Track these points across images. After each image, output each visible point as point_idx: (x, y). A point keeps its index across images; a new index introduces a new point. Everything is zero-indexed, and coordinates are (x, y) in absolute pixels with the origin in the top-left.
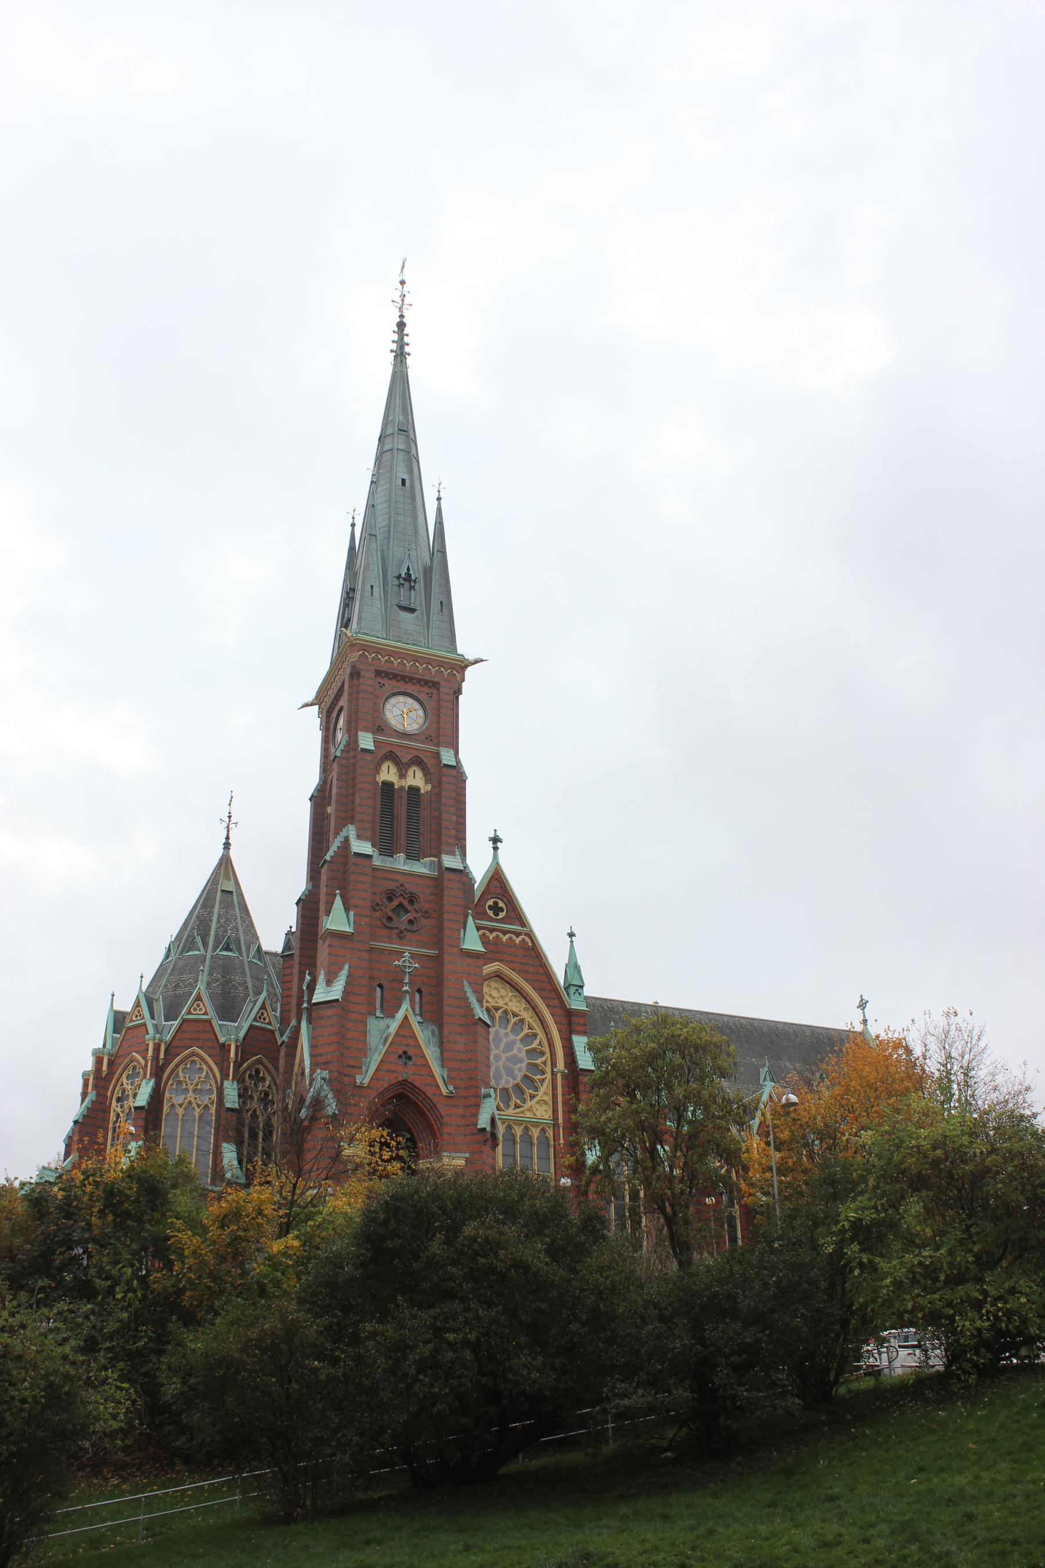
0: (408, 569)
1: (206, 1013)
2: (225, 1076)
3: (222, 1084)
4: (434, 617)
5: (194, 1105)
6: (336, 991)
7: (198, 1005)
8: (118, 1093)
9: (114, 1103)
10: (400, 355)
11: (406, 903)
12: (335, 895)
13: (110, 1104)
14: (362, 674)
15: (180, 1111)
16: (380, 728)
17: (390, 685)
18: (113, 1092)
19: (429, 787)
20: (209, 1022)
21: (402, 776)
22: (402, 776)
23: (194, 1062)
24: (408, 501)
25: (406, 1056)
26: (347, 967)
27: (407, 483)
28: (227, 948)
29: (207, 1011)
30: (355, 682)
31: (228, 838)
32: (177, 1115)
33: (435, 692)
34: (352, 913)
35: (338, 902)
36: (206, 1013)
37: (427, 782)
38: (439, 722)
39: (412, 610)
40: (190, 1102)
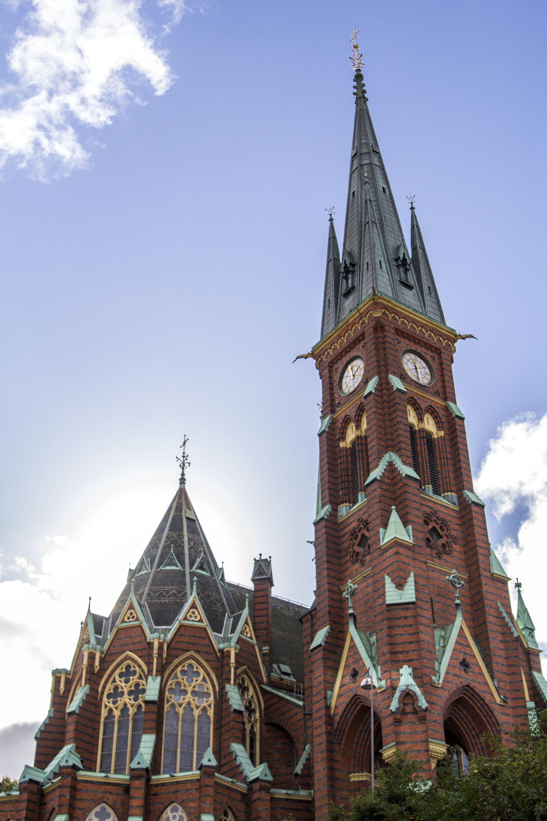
0: (404, 254)
1: (201, 621)
2: (223, 679)
3: (222, 688)
4: (427, 297)
5: (193, 706)
6: (409, 594)
7: (194, 613)
8: (109, 688)
9: (105, 699)
10: (361, 98)
11: (438, 527)
12: (390, 512)
13: (101, 699)
14: (386, 328)
15: (181, 711)
16: (403, 377)
17: (405, 344)
18: (104, 688)
19: (442, 433)
20: (205, 629)
21: (421, 420)
22: (421, 420)
23: (190, 666)
24: (390, 205)
25: (465, 664)
26: (412, 574)
27: (387, 191)
28: (201, 567)
29: (198, 618)
30: (379, 334)
31: (183, 474)
32: (177, 714)
33: (436, 356)
34: (410, 527)
35: (394, 517)
36: (201, 621)
37: (439, 428)
38: (443, 381)
39: (410, 287)
40: (189, 703)
